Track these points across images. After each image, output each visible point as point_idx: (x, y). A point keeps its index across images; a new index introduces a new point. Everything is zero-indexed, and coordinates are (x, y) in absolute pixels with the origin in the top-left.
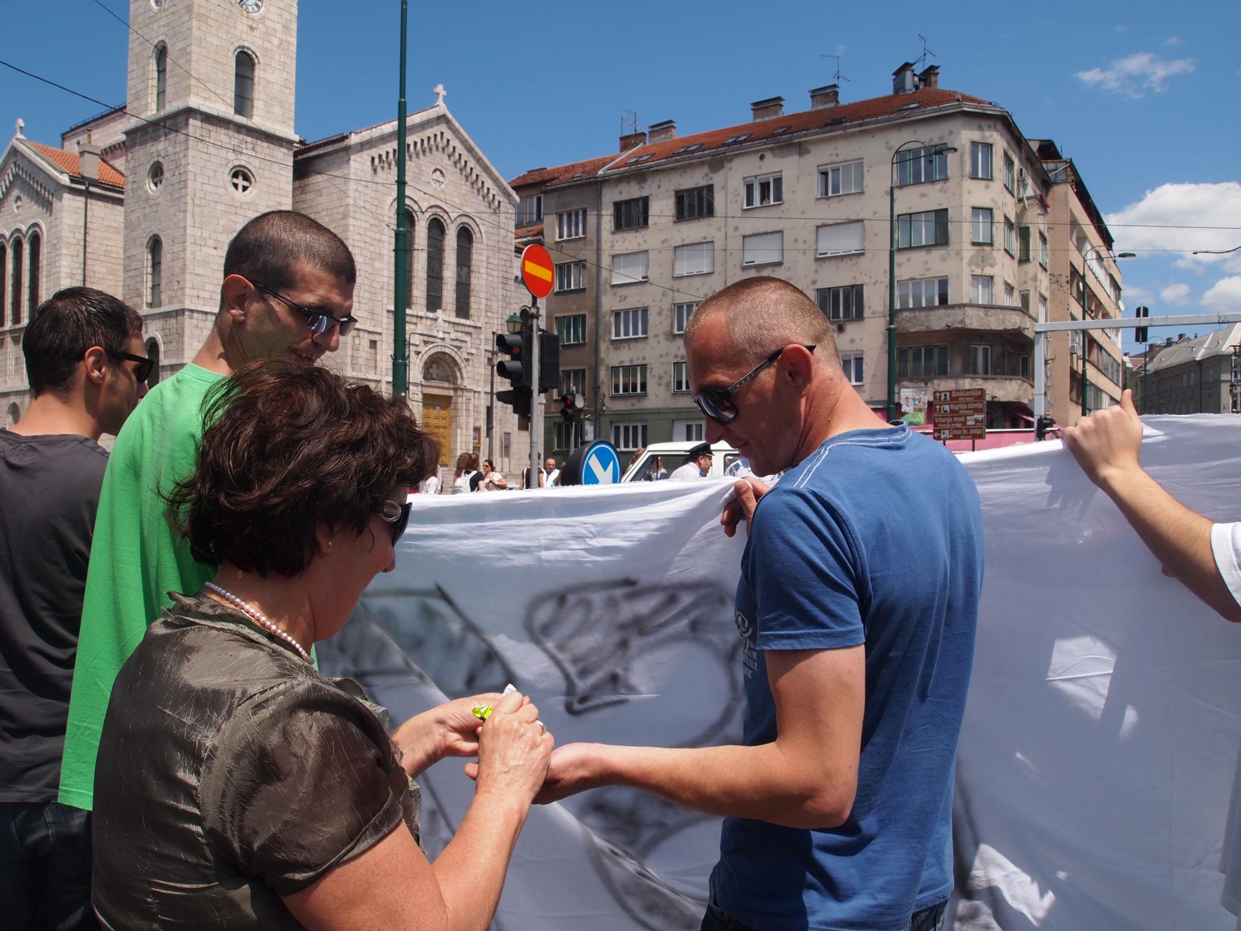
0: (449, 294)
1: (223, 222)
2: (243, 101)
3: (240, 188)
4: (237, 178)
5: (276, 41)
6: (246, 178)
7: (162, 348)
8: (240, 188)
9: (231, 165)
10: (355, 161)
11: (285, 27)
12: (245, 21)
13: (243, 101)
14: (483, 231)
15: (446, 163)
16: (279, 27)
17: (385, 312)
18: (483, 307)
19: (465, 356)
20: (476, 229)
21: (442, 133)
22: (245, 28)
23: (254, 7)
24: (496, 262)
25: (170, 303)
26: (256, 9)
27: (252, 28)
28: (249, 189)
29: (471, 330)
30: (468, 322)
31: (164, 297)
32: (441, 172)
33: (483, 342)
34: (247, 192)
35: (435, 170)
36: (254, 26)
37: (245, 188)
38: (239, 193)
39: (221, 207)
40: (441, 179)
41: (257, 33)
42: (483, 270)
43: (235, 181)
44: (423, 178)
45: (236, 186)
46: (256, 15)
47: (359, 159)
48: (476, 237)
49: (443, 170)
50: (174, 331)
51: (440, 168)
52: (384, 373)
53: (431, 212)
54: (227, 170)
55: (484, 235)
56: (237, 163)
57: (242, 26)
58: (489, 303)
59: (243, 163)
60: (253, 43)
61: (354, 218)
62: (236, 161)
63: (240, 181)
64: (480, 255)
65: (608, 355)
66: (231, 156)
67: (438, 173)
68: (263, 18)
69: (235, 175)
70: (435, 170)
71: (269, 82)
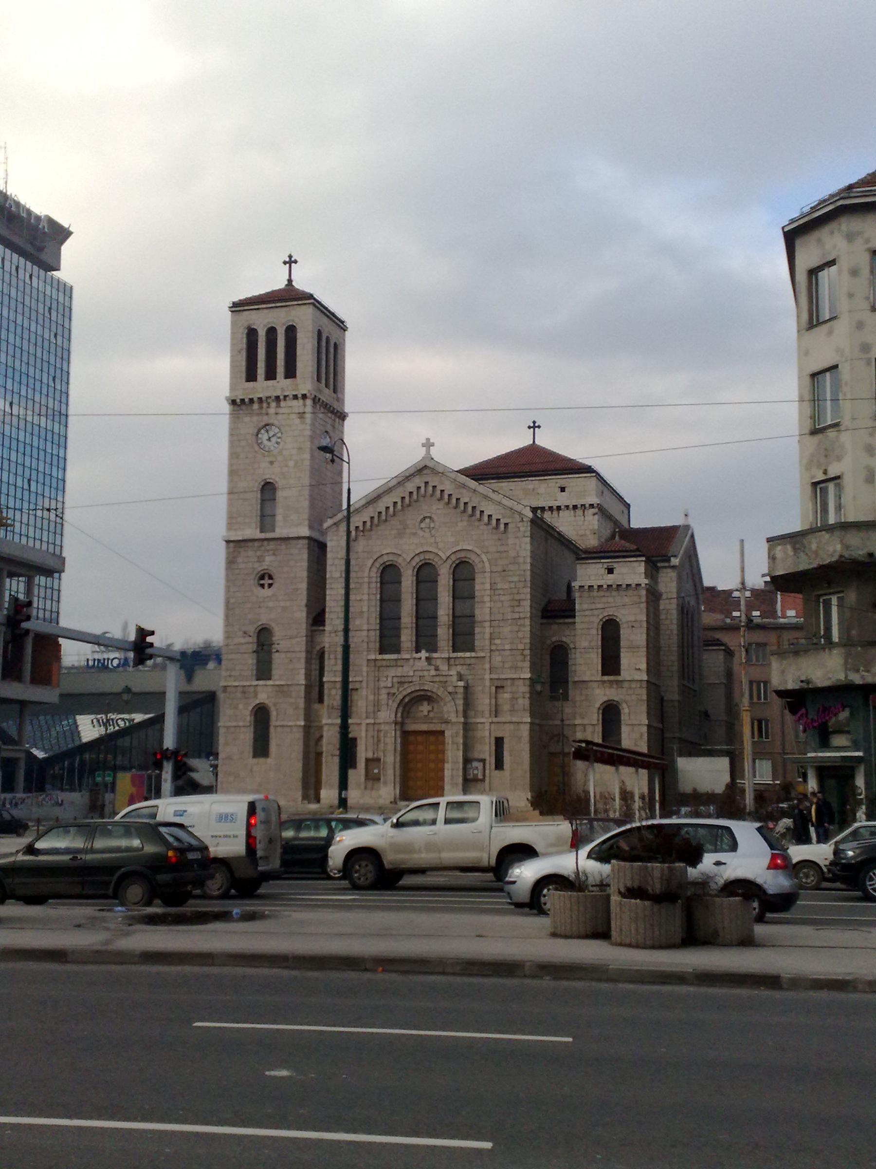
0: (444, 633)
1: (250, 616)
2: (266, 520)
3: (266, 586)
5: (291, 463)
6: (271, 578)
8: (266, 586)
10: (331, 540)
11: (300, 449)
12: (268, 459)
13: (266, 520)
14: (485, 559)
15: (436, 509)
16: (294, 452)
17: (365, 663)
18: (487, 636)
19: (450, 689)
20: (477, 560)
21: (426, 483)
24: (506, 586)
28: (274, 586)
29: (473, 661)
30: (473, 654)
32: (430, 518)
33: (488, 671)
35: (425, 518)
36: (274, 459)
37: (270, 585)
38: (267, 592)
39: (249, 605)
40: (432, 525)
41: (276, 464)
42: (487, 599)
43: (262, 582)
44: (408, 531)
45: (262, 586)
47: (335, 538)
48: (478, 567)
49: (433, 516)
51: (428, 515)
52: (364, 715)
53: (417, 559)
54: (253, 576)
55: (487, 565)
56: (260, 569)
57: (265, 465)
58: (497, 630)
59: (266, 567)
60: (272, 474)
61: (332, 588)
62: (259, 568)
63: (266, 582)
64: (482, 586)
66: (256, 565)
67: (427, 520)
68: (281, 452)
69: (262, 577)
70: (425, 518)
71: (286, 498)
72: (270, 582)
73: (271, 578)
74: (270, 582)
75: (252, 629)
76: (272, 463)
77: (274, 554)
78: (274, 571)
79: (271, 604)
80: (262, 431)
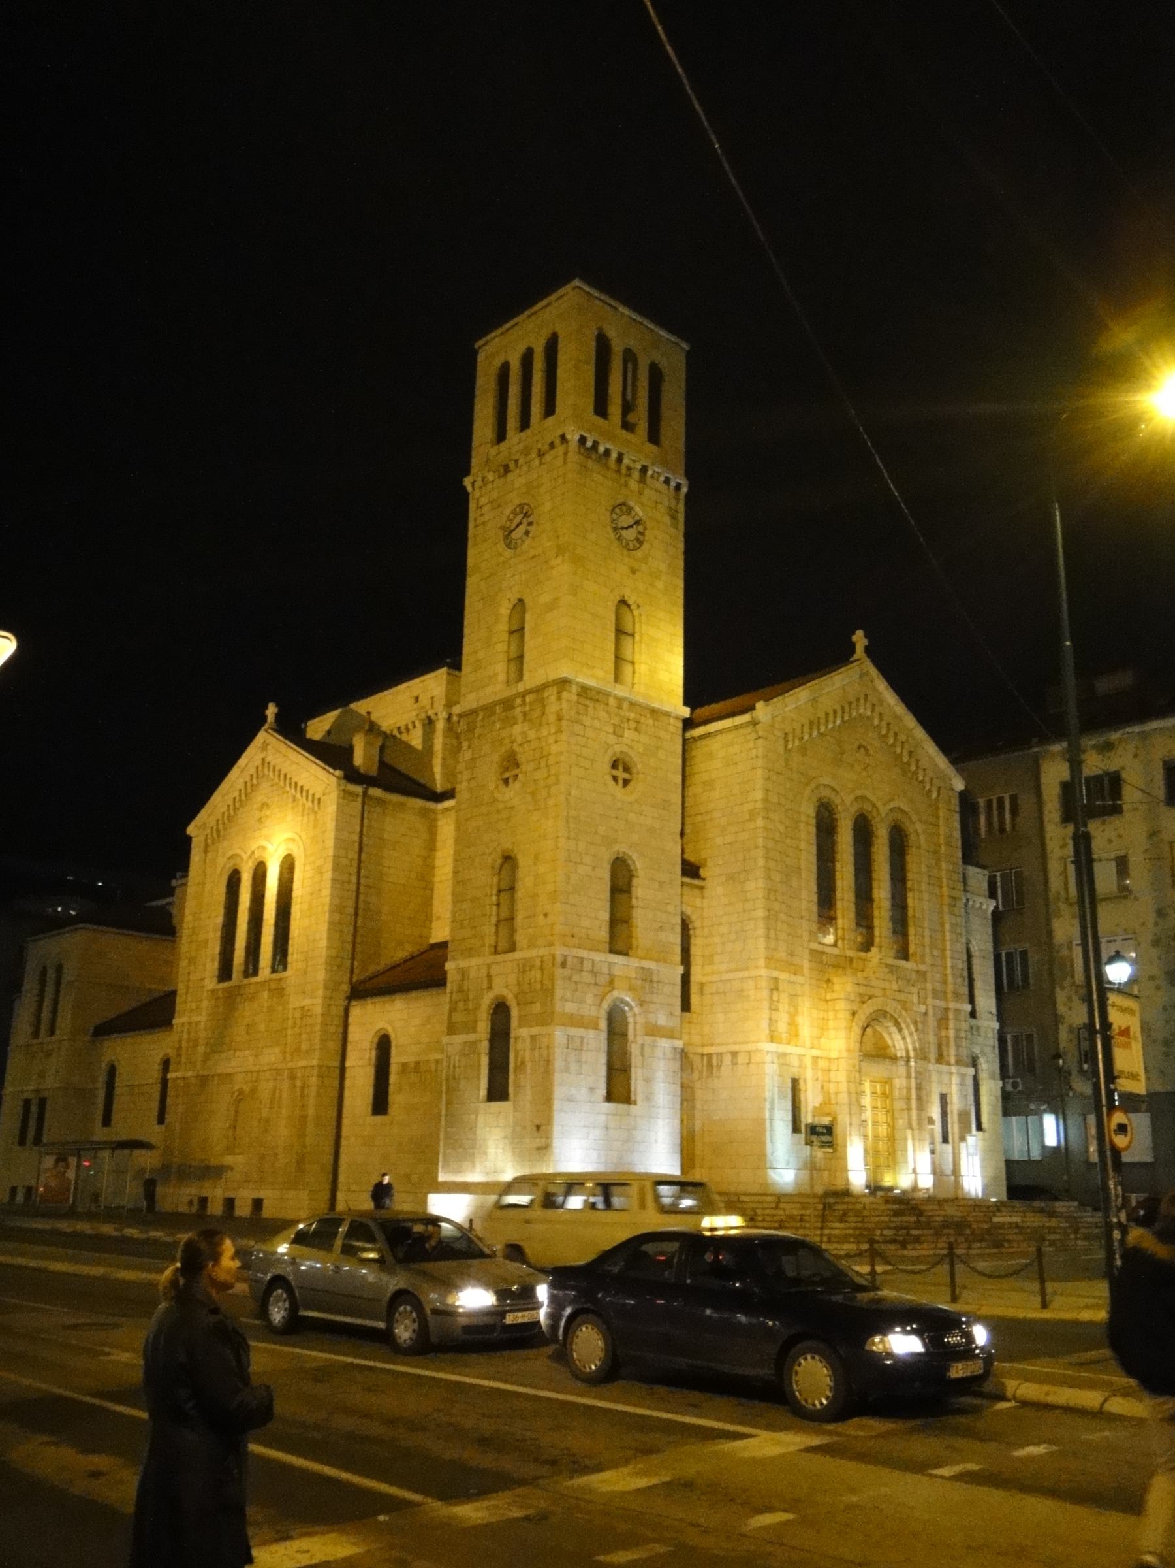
1: (602, 830)
3: (621, 782)
4: (618, 769)
6: (627, 769)
7: (515, 1013)
9: (610, 752)
22: (625, 569)
23: (635, 542)
25: (532, 945)
26: (638, 545)
27: (634, 571)
31: (521, 938)
34: (629, 787)
37: (626, 782)
38: (618, 790)
43: (615, 772)
45: (615, 779)
46: (639, 554)
50: (538, 986)
59: (625, 749)
63: (621, 775)
65: (1070, 1009)
66: (612, 739)
69: (614, 765)
72: (626, 776)
73: (627, 769)
74: (626, 776)
75: (607, 857)
76: (634, 571)
77: (636, 729)
78: (635, 757)
79: (632, 817)
80: (617, 510)
